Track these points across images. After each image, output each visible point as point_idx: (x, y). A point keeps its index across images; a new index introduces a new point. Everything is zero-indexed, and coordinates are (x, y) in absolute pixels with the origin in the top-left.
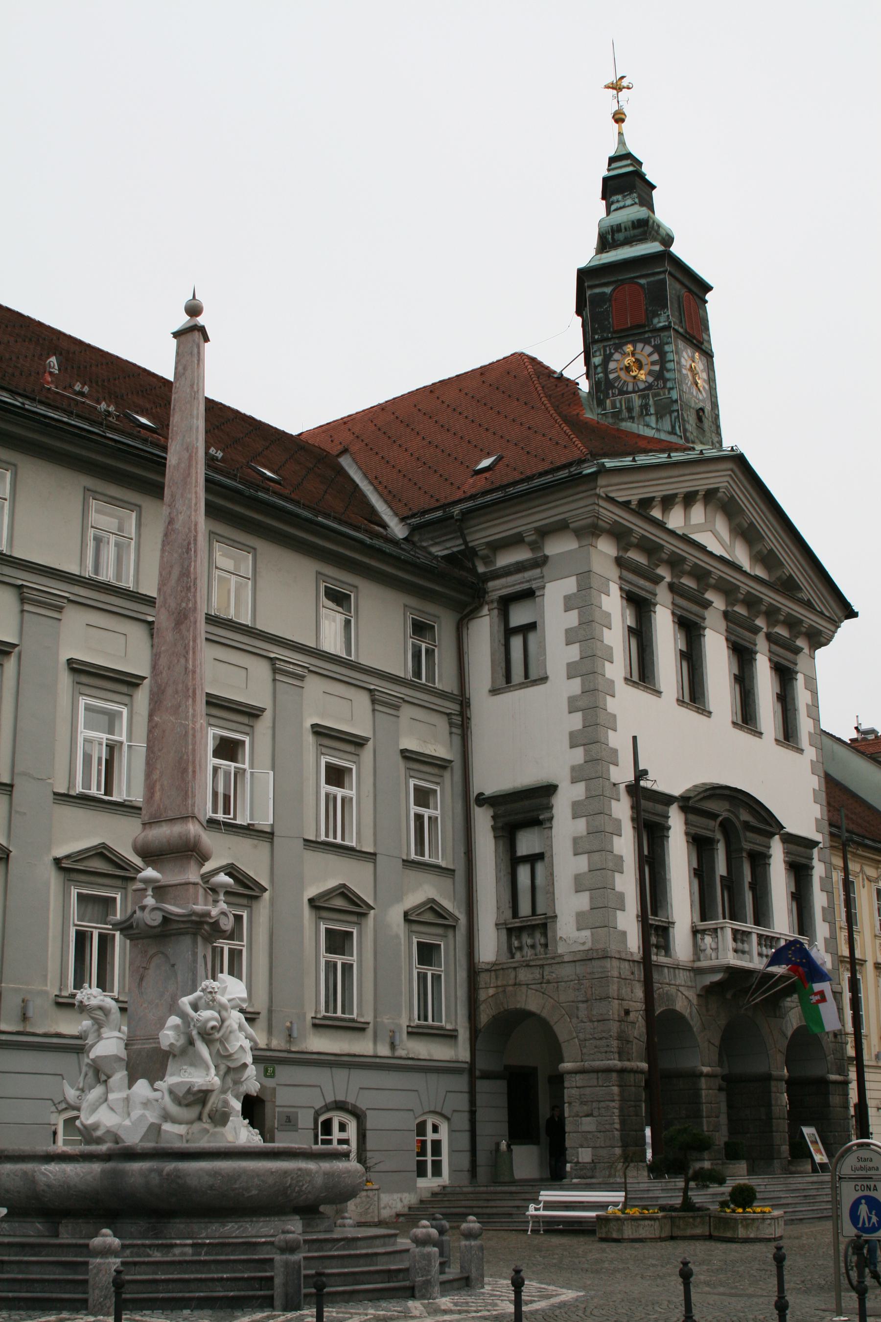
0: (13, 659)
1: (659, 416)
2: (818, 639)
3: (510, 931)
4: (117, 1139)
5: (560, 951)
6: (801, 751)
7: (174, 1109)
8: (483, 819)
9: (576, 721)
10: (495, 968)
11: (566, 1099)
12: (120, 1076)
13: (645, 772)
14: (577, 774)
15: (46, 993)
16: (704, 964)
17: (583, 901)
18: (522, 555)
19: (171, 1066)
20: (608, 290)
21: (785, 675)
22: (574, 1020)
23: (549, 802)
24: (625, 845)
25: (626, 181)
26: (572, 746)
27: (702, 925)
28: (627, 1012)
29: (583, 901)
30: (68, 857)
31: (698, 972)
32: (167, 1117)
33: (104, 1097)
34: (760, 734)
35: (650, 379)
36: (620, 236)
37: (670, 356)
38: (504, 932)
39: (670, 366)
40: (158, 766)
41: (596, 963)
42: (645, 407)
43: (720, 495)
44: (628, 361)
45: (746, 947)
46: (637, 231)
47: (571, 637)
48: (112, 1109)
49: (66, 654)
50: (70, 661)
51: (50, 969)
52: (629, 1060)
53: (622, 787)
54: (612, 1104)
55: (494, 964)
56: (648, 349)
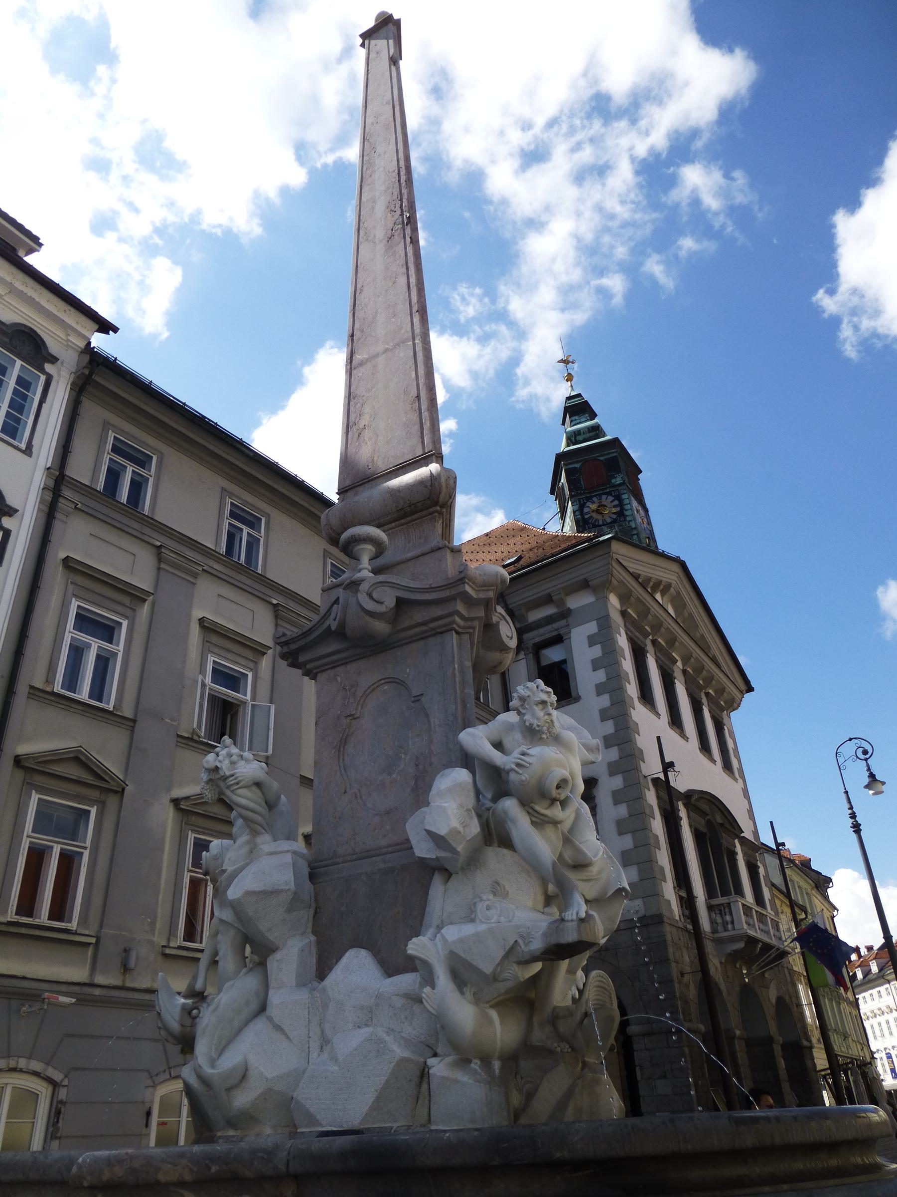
0: (146, 606)
2: (733, 705)
6: (736, 780)
7: (463, 1013)
9: (609, 728)
11: (637, 1062)
13: (671, 764)
14: (614, 769)
15: (151, 942)
18: (549, 611)
19: (441, 898)
24: (657, 826)
27: (715, 902)
28: (682, 974)
30: (187, 798)
31: (719, 942)
32: (439, 1036)
33: (254, 1006)
35: (615, 516)
36: (580, 438)
37: (627, 501)
39: (628, 507)
40: (367, 409)
43: (672, 589)
46: (592, 434)
47: (596, 665)
48: (278, 1028)
49: (198, 613)
50: (201, 621)
51: (159, 915)
52: (690, 1021)
53: (649, 778)
56: (611, 498)
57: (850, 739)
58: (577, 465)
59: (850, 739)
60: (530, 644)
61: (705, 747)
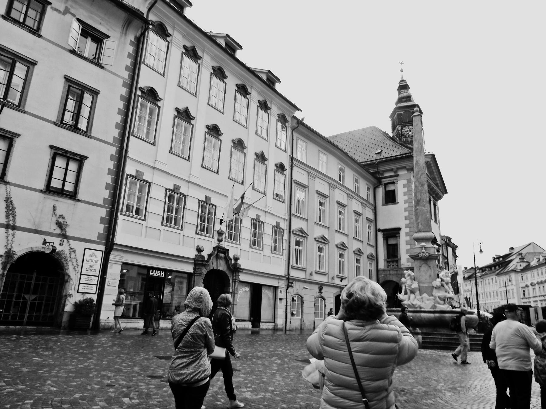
4: (421, 308)
5: (402, 267)
8: (380, 235)
10: (384, 270)
12: (418, 293)
14: (407, 226)
18: (392, 174)
20: (402, 112)
21: (435, 206)
25: (403, 86)
26: (406, 219)
36: (404, 100)
44: (407, 129)
58: (402, 112)
60: (384, 183)
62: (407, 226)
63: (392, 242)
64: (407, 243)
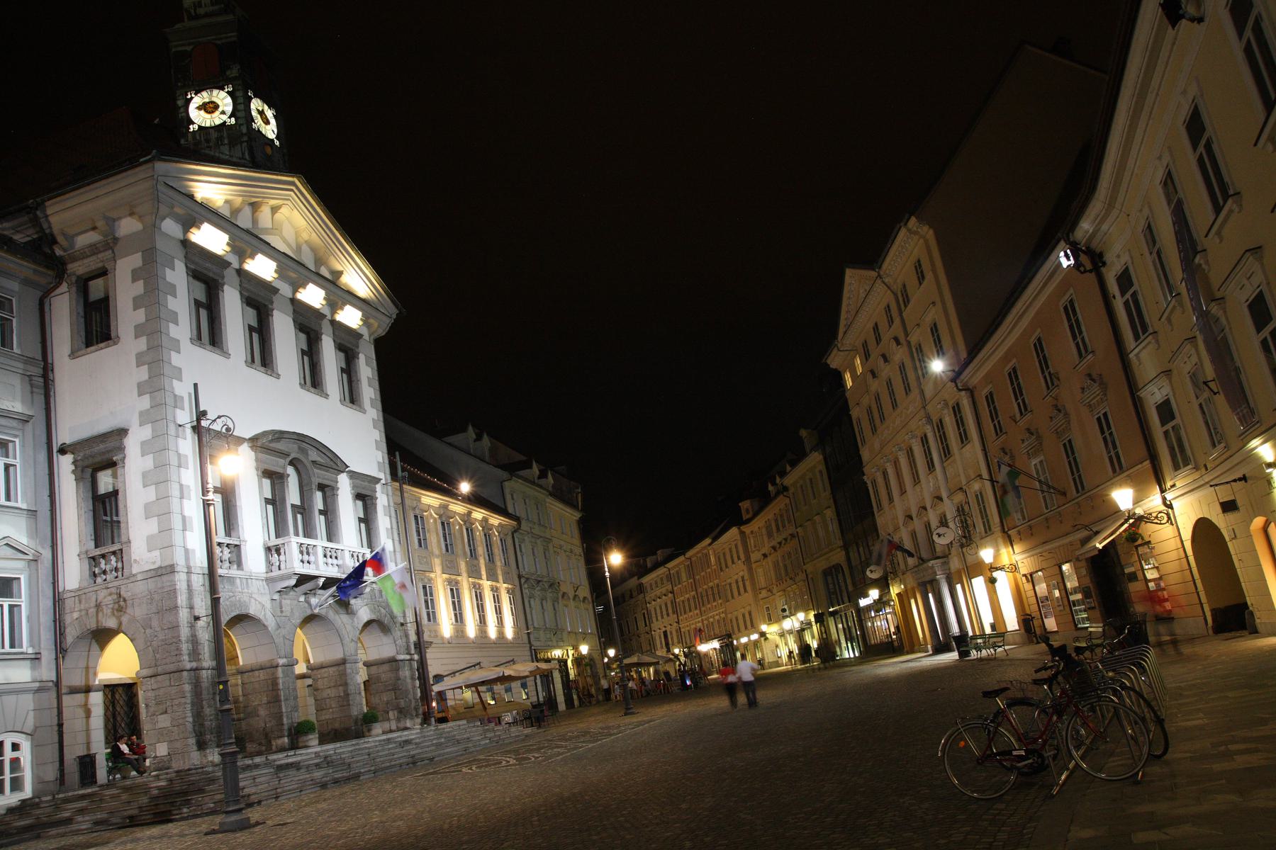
1: (232, 145)
3: (94, 560)
6: (364, 412)
8: (65, 464)
10: (79, 594)
16: (276, 573)
17: (152, 526)
22: (148, 631)
23: (122, 443)
27: (274, 541)
28: (197, 618)
29: (152, 526)
34: (327, 396)
38: (86, 562)
41: (165, 578)
42: (220, 139)
45: (312, 558)
47: (137, 303)
54: (183, 700)
55: (79, 590)
56: (223, 94)
57: (219, 417)
58: (189, 48)
59: (219, 417)
61: (314, 380)
62: (145, 418)
63: (105, 482)
64: (147, 479)
